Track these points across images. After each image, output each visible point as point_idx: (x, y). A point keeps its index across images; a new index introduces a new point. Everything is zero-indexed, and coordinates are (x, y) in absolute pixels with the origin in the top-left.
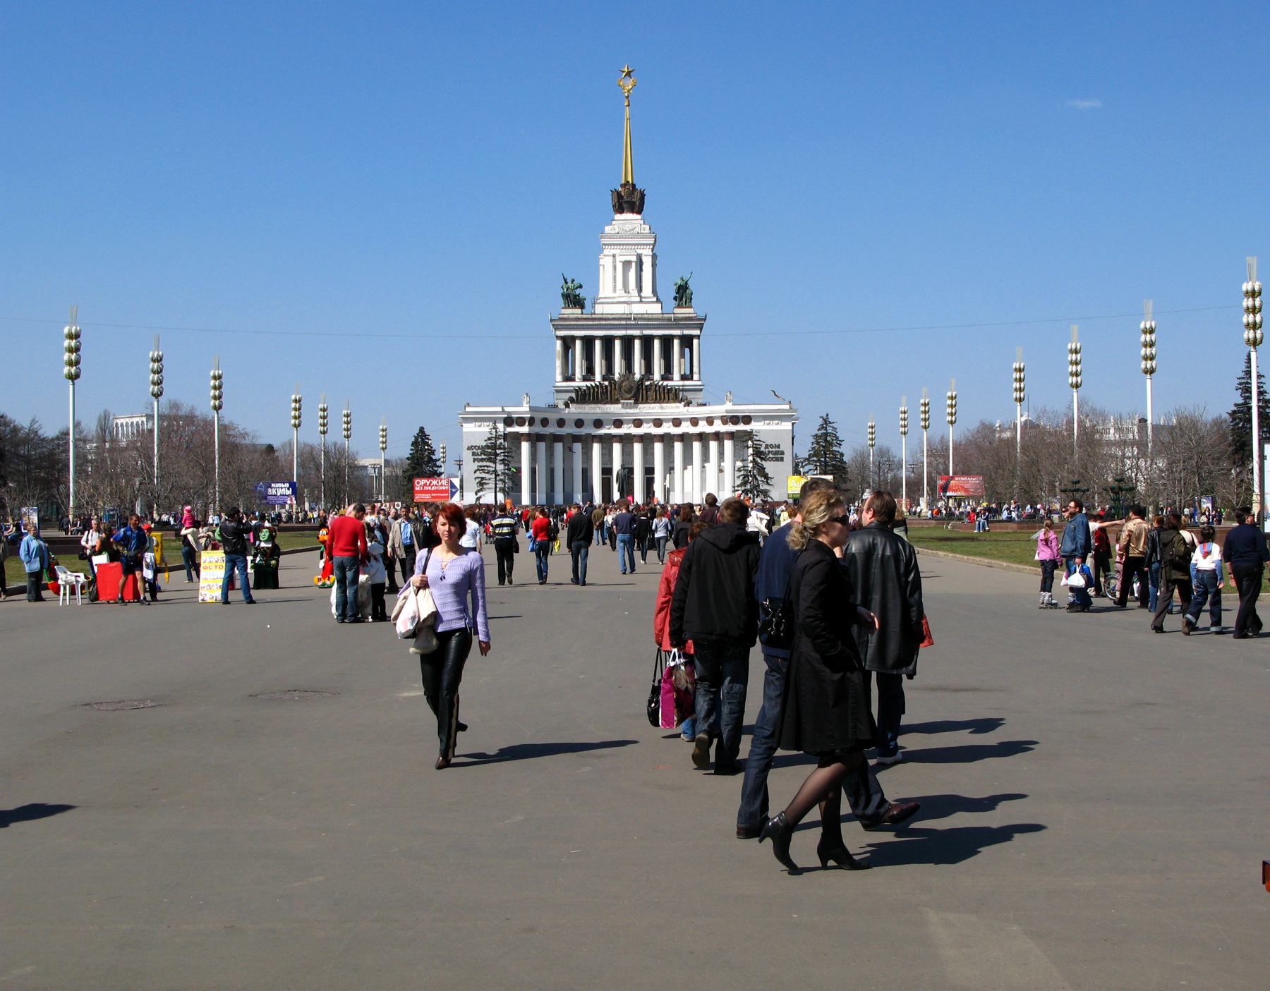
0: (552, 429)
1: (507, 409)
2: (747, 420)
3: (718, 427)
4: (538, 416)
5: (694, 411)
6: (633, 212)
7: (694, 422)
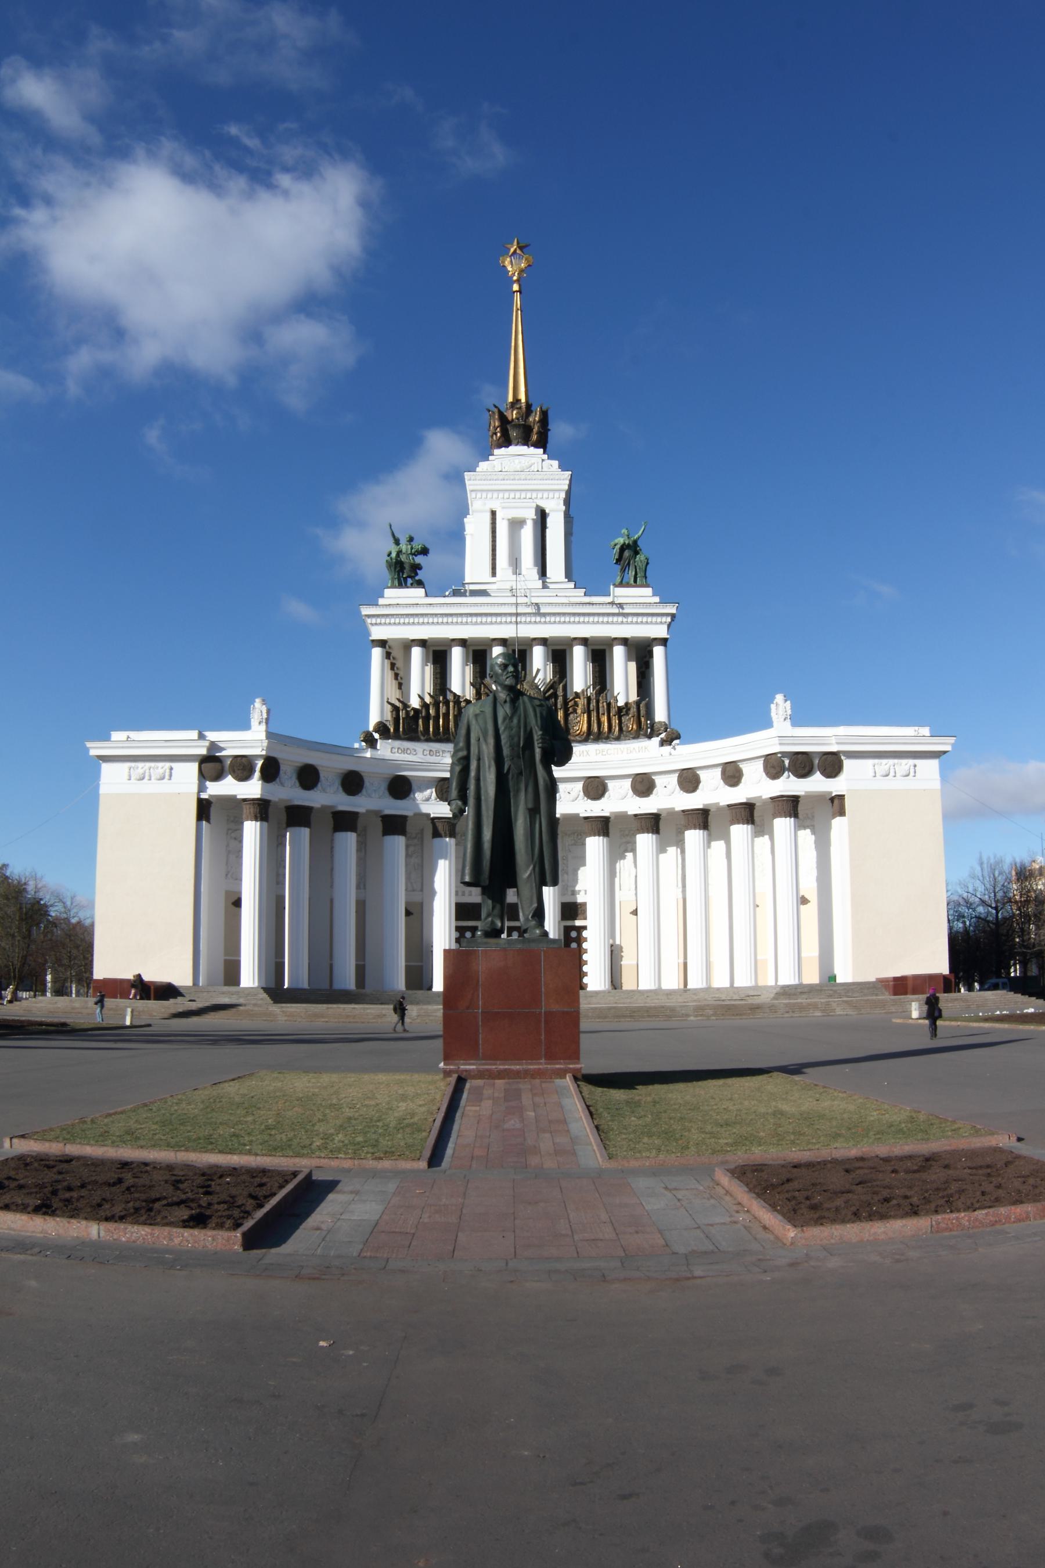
0: (327, 797)
1: (212, 736)
2: (832, 764)
3: (757, 786)
4: (291, 759)
5: (685, 755)
6: (526, 441)
7: (689, 780)
